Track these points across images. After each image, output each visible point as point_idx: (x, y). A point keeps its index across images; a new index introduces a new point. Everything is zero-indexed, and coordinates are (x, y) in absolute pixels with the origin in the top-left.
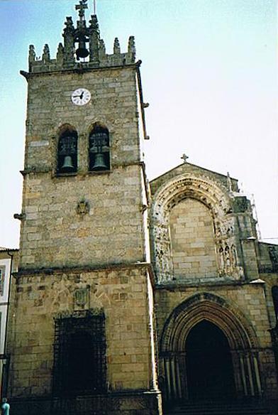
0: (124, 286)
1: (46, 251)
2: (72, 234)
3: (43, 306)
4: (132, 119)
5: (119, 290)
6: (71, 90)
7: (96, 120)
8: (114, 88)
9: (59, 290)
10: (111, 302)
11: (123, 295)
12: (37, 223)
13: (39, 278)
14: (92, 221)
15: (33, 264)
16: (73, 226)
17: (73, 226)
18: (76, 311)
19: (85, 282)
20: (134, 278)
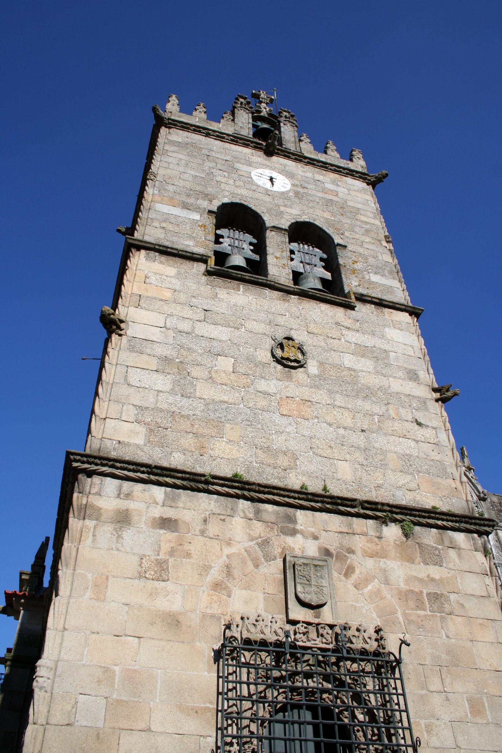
0: (435, 572)
1: (185, 425)
2: (263, 403)
3: (169, 585)
4: (380, 241)
5: (421, 580)
6: (250, 165)
7: (305, 218)
8: (337, 192)
9: (229, 543)
10: (404, 614)
11: (435, 597)
12: (160, 351)
13: (158, 492)
14: (317, 387)
15: (138, 446)
16: (262, 385)
17: (262, 385)
18: (294, 623)
19: (316, 538)
20: (459, 555)
